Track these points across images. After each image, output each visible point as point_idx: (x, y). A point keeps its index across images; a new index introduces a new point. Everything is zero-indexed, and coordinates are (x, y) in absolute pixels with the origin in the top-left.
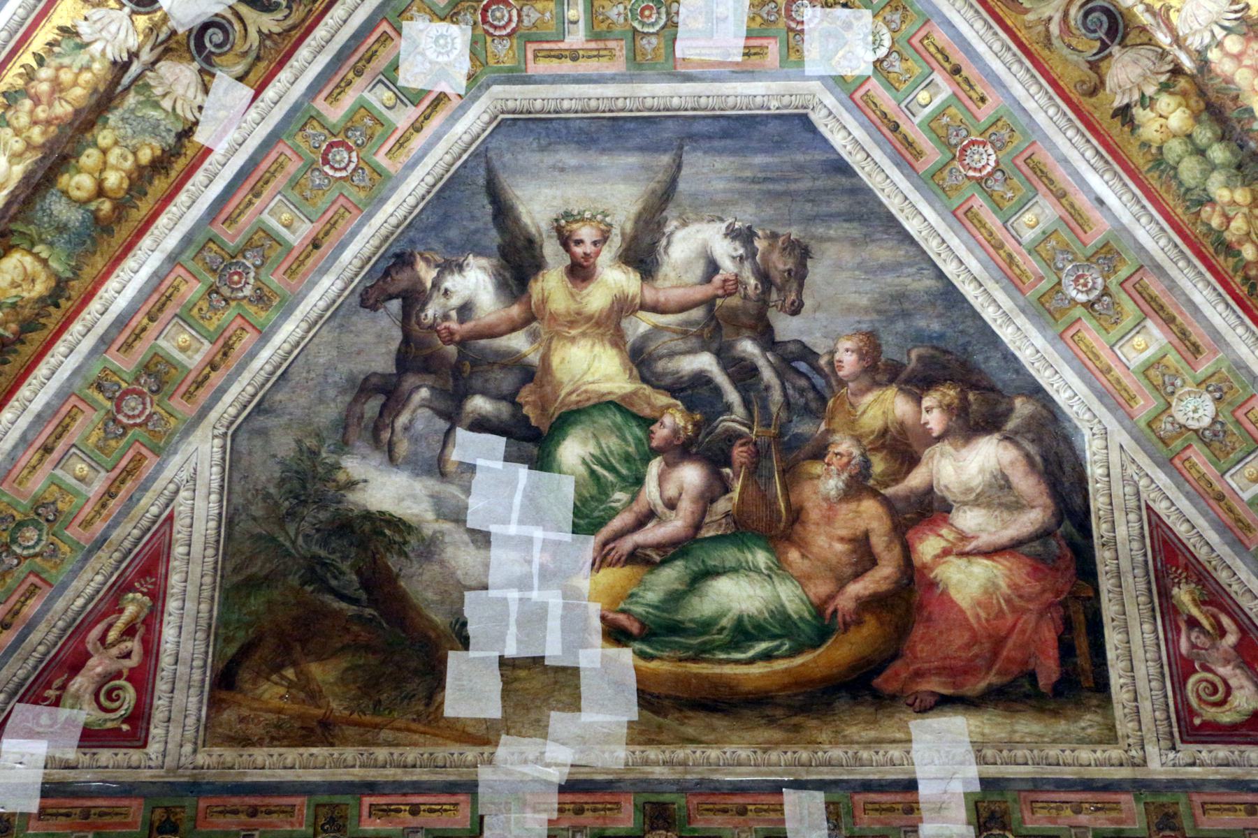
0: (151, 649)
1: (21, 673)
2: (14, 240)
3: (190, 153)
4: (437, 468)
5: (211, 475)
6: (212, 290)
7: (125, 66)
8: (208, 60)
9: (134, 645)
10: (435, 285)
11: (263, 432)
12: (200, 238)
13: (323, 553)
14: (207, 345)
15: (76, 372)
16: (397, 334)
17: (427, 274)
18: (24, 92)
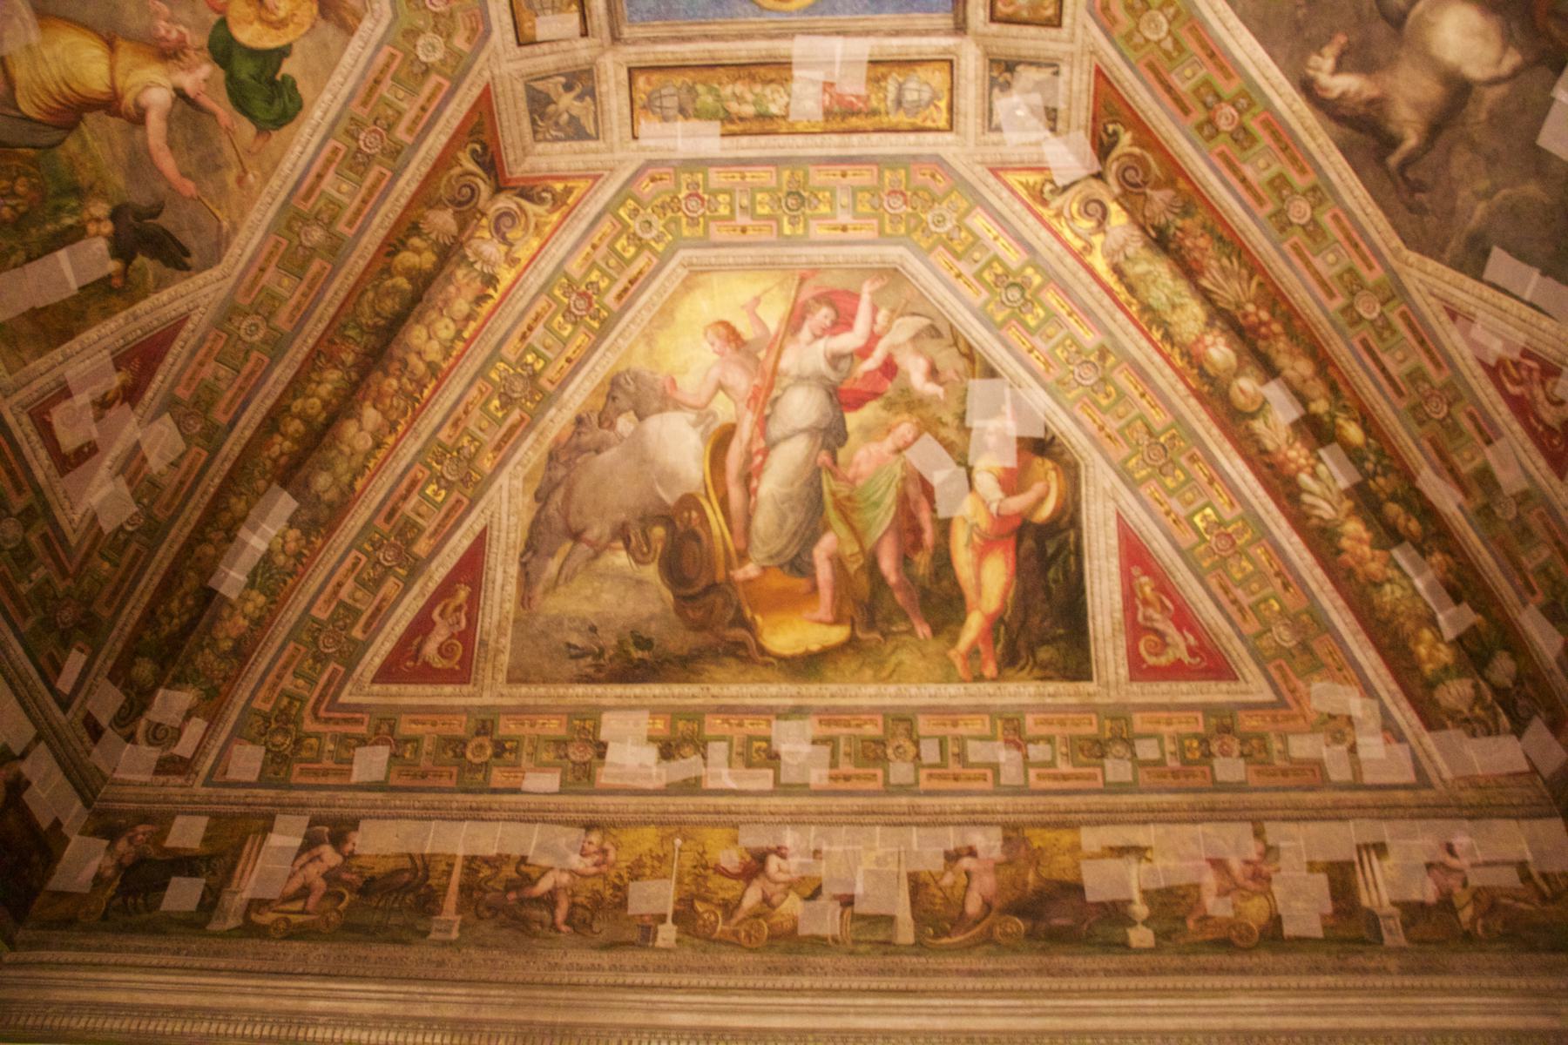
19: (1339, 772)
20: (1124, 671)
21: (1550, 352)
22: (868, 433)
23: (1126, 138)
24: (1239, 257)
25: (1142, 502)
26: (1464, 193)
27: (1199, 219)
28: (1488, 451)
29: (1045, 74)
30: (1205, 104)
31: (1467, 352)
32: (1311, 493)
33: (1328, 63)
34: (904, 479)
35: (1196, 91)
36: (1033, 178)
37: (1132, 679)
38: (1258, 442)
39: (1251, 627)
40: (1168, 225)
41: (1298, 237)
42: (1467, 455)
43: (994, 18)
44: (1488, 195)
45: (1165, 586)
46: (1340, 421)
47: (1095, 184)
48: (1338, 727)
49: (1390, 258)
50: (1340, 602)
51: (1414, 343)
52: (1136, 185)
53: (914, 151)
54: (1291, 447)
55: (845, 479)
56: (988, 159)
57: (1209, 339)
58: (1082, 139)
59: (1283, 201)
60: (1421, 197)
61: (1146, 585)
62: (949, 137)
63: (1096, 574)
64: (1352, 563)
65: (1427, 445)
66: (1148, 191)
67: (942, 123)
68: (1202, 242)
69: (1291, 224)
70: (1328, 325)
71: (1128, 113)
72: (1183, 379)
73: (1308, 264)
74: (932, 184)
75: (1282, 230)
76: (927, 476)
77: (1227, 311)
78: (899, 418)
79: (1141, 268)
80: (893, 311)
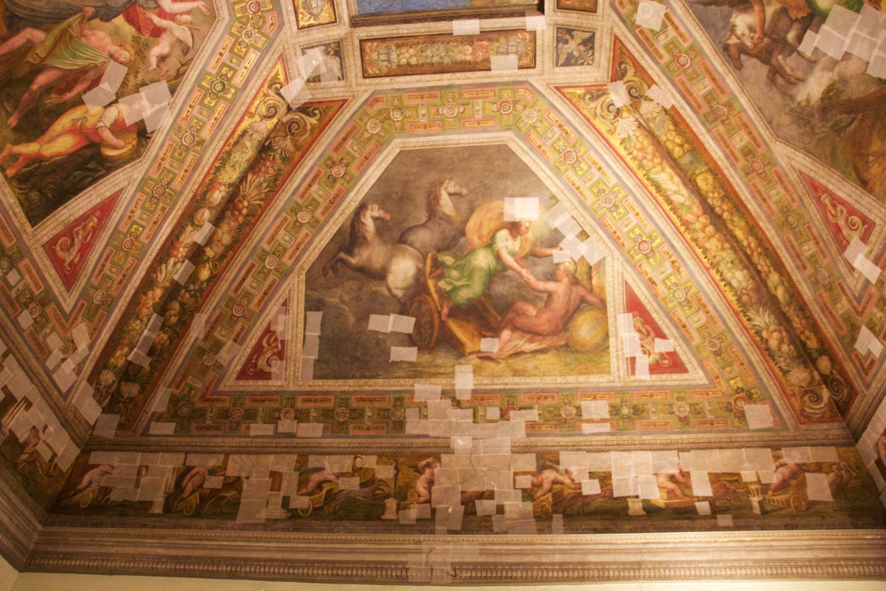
0: (843, 203)
1: (835, 247)
2: (692, 179)
3: (672, 113)
4: (812, 63)
5: (789, 150)
6: (723, 122)
7: (640, 124)
8: (642, 96)
9: (839, 207)
10: (739, 38)
11: (779, 125)
12: (703, 119)
13: (831, 123)
14: (742, 132)
15: (740, 178)
16: (755, 60)
17: (733, 40)
18: (640, 161)
19: (50, 364)
20: (46, 239)
21: (289, 351)
22: (116, 33)
23: (314, 121)
24: (270, 191)
25: (133, 197)
26: (339, 291)
27: (283, 167)
28: (231, 342)
29: (338, 73)
30: (342, 159)
31: (271, 316)
32: (166, 267)
33: (376, 214)
34: (96, 66)
35: (348, 153)
36: (281, 77)
37: (43, 246)
38: (181, 232)
39: (95, 282)
40: (274, 151)
41: (291, 219)
42: (223, 333)
43: (362, 41)
44: (342, 301)
45: (96, 232)
46: (207, 266)
47: (285, 107)
48: (70, 346)
49: (298, 266)
50: (123, 308)
51: (263, 290)
52: (290, 130)
53: (284, 11)
54: (184, 247)
55: (82, 30)
56: (287, 52)
57: (222, 188)
58: (307, 97)
59: (306, 207)
60: (331, 273)
61: (93, 222)
62: (295, 29)
63: (87, 195)
64: (143, 302)
65: (218, 312)
66: (289, 137)
67: (302, 23)
68: (271, 171)
69: (296, 214)
70: (253, 245)
71: (327, 119)
72: (200, 186)
73: (279, 227)
74: (268, 25)
75: (292, 211)
76: (103, 78)
77: (239, 191)
78: (130, 49)
79: (248, 144)
80: (191, 23)
